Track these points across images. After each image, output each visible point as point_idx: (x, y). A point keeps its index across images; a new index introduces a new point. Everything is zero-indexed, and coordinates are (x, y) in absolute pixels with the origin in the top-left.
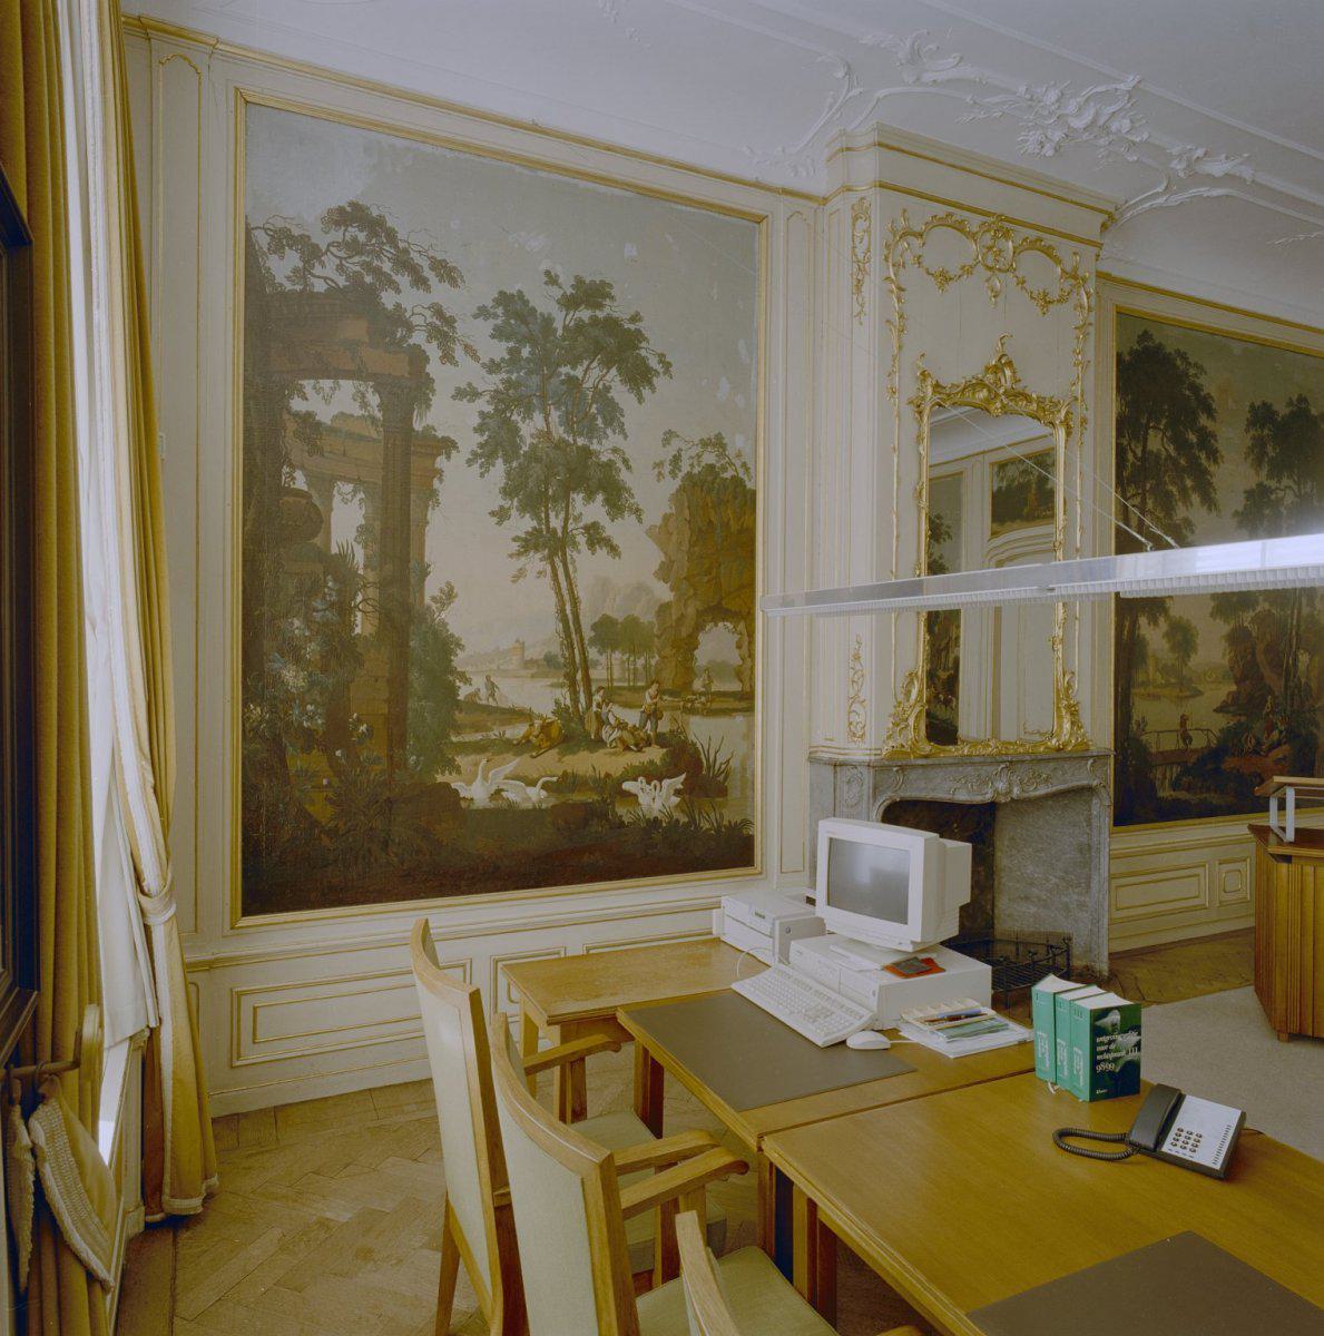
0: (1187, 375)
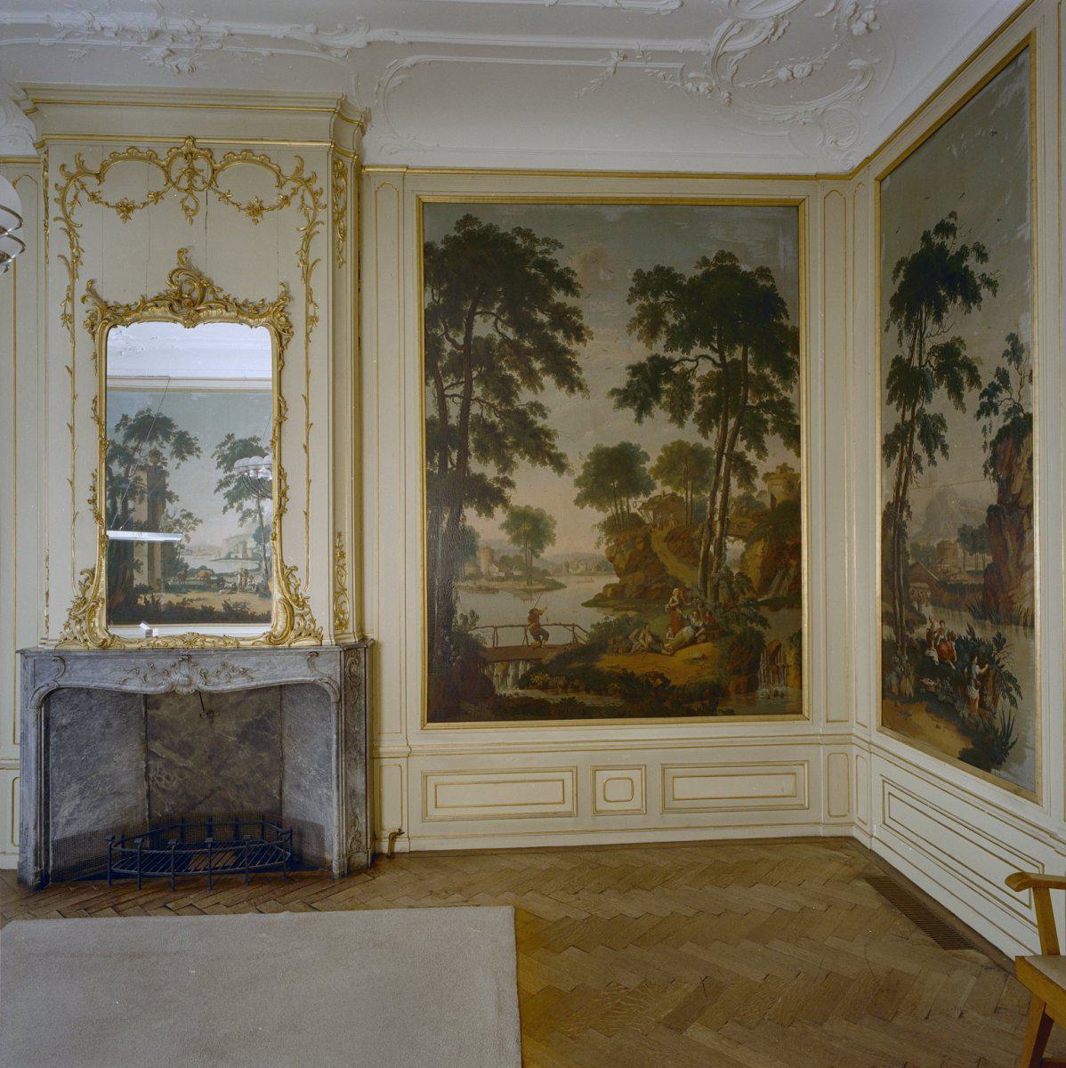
0: (533, 253)
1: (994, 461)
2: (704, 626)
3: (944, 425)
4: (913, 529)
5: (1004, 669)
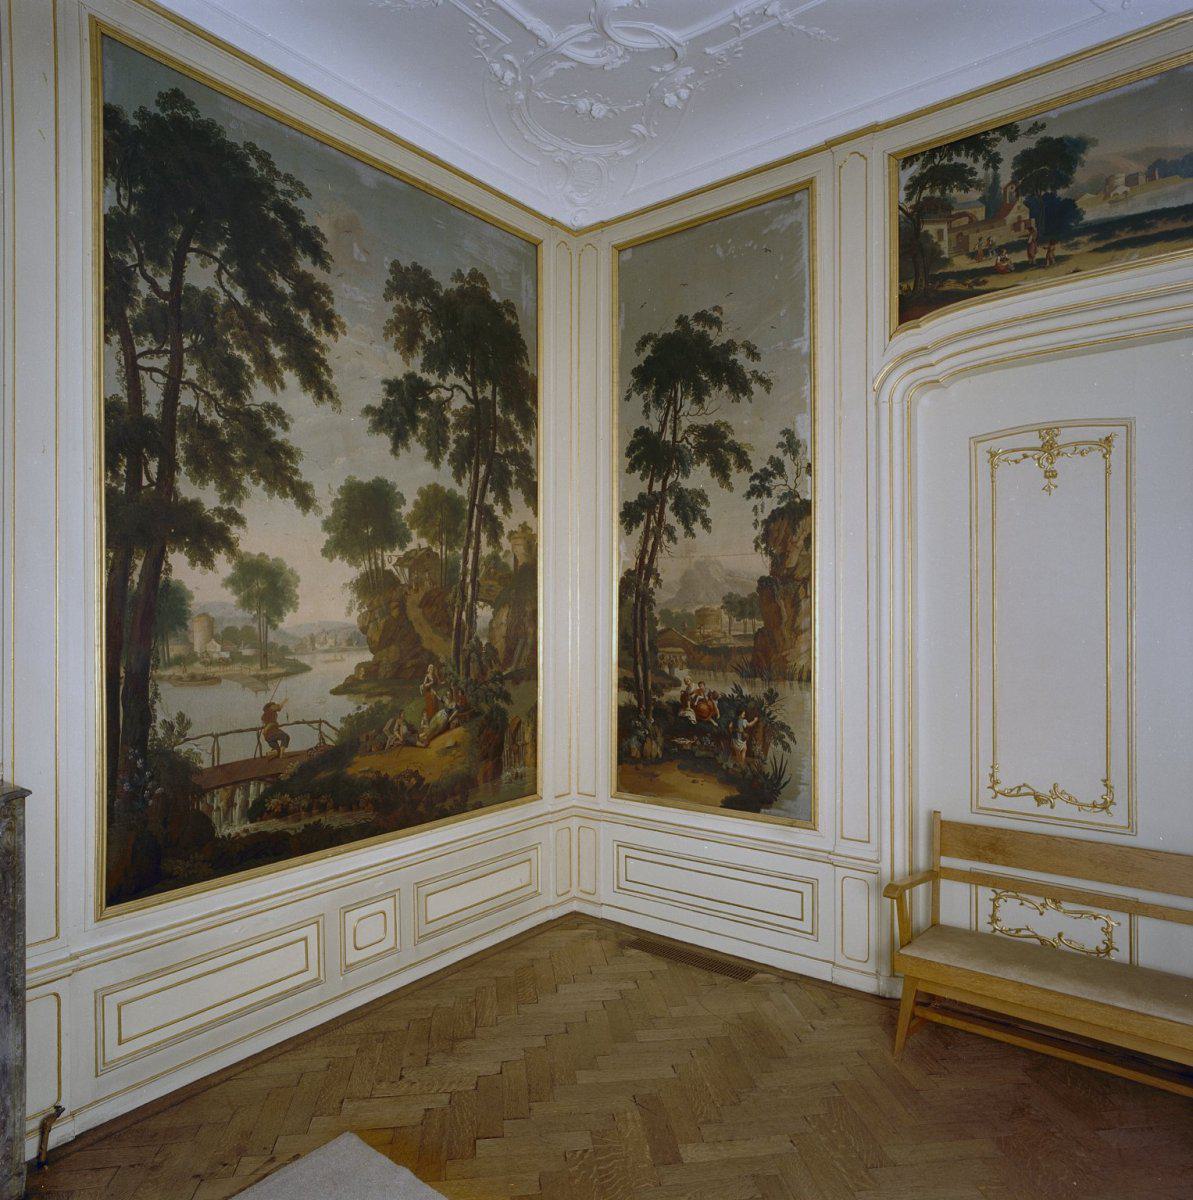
0: (273, 190)
1: (766, 537)
2: (457, 707)
3: (705, 500)
4: (662, 597)
5: (775, 720)
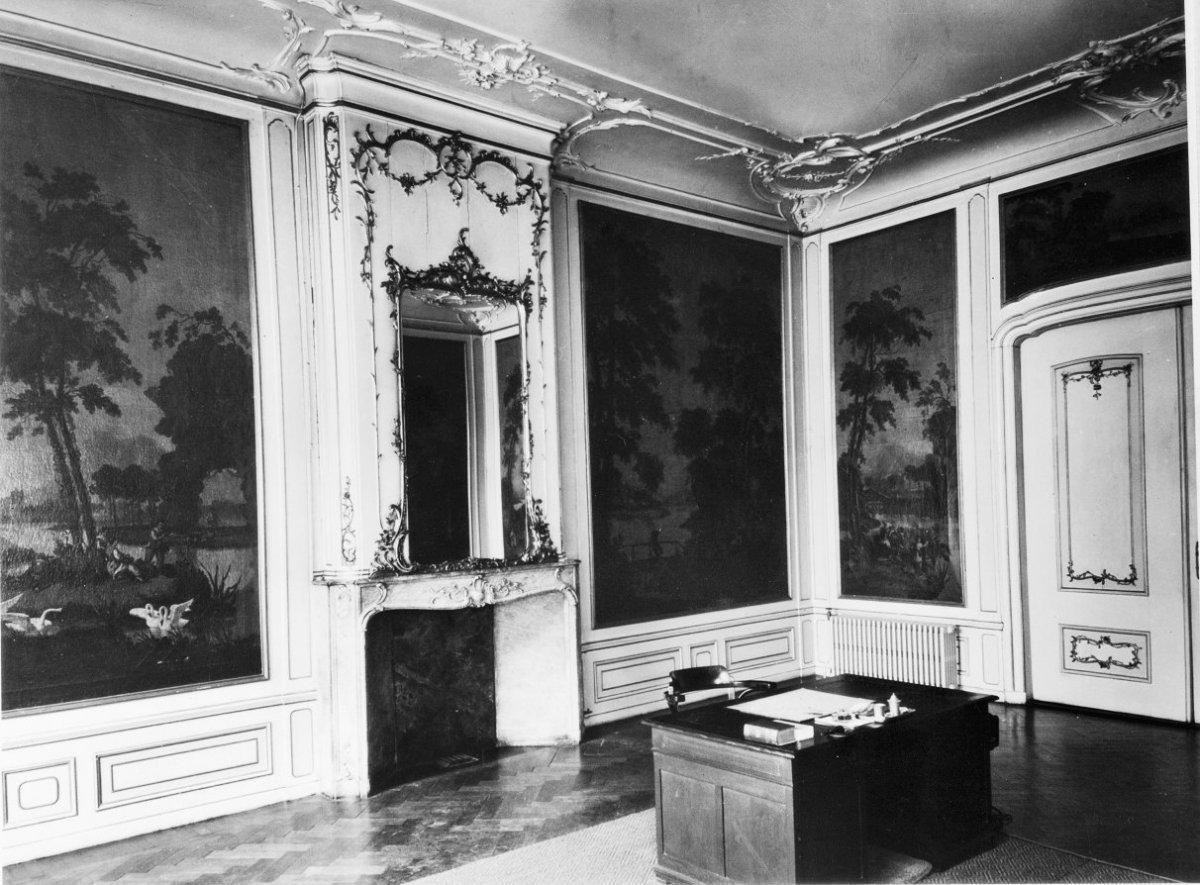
4: (866, 469)
